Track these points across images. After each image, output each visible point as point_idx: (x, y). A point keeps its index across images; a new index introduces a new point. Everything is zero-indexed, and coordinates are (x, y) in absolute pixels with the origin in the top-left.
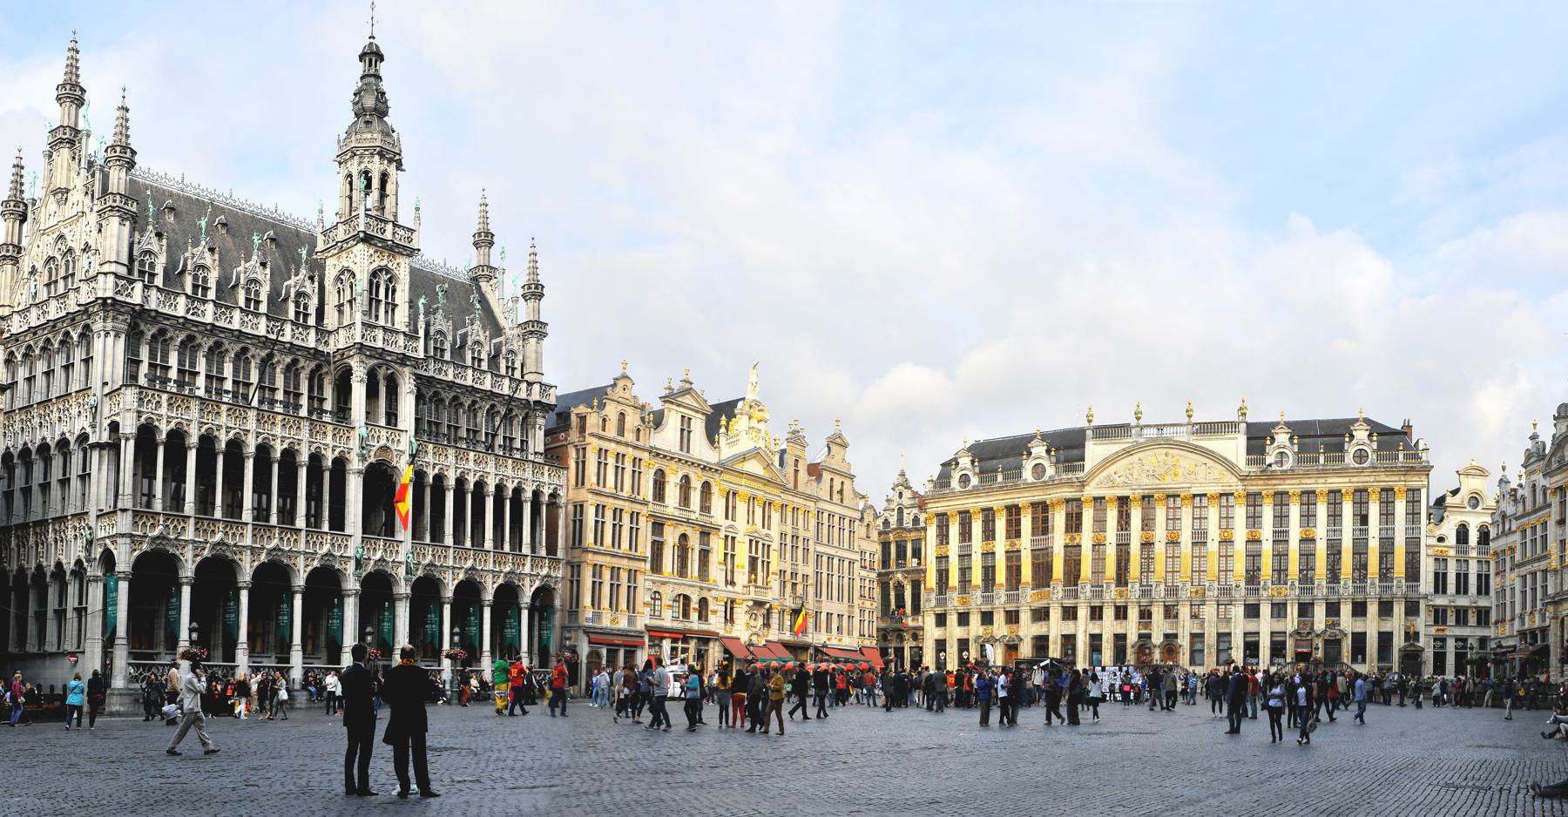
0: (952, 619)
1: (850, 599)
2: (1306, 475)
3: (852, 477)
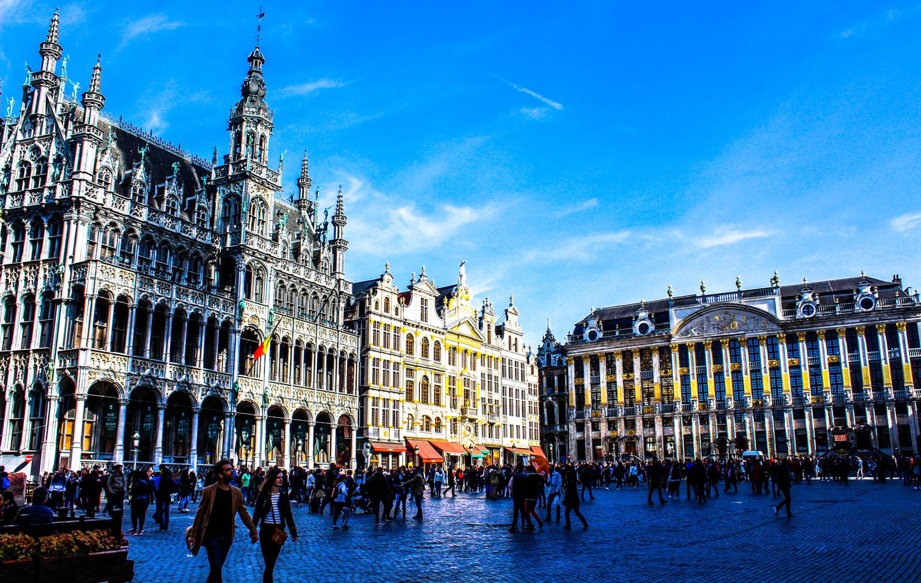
1: (524, 416)
2: (828, 319)
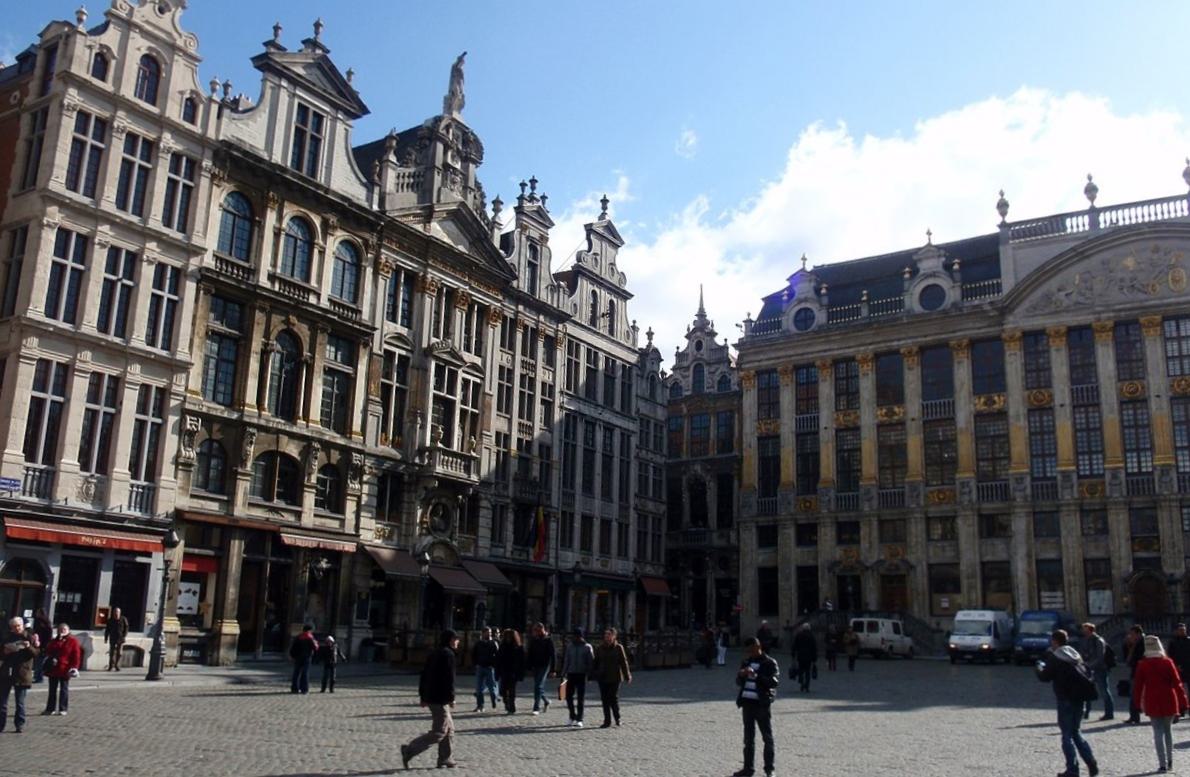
0: (788, 535)
3: (626, 296)
